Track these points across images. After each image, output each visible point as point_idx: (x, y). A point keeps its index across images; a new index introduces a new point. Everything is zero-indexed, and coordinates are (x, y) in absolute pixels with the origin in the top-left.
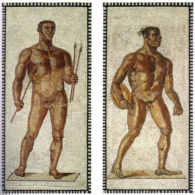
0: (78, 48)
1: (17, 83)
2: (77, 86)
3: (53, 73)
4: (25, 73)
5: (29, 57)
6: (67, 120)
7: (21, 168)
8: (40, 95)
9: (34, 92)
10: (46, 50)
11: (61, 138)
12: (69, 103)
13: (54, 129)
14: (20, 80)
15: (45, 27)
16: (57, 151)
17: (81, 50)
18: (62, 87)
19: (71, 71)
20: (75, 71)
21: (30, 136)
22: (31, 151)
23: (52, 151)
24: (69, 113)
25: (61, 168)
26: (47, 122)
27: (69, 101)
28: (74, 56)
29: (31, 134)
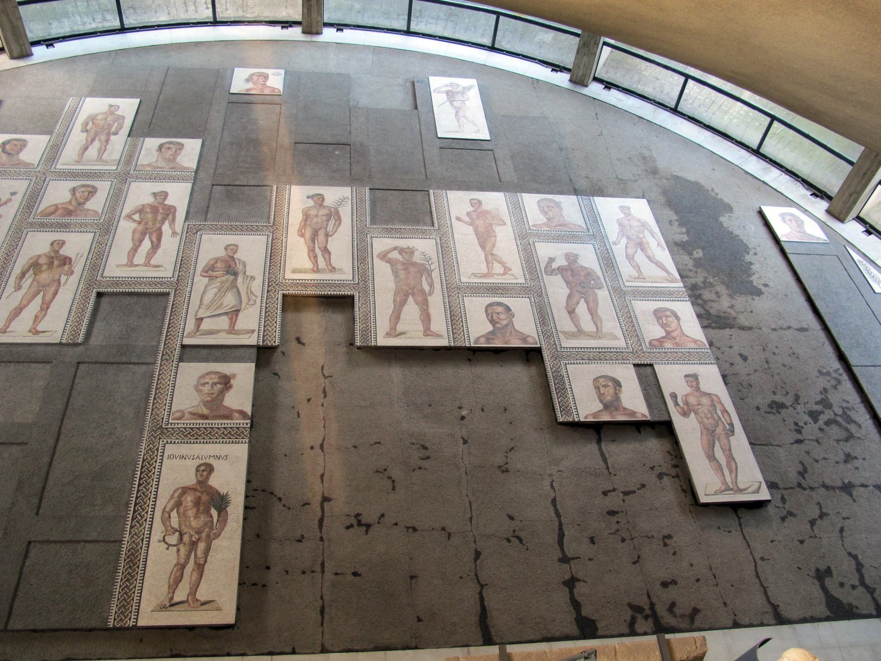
1: (21, 275)
2: (71, 278)
3: (54, 269)
5: (38, 260)
6: (57, 297)
9: (34, 280)
11: (48, 308)
12: (61, 287)
13: (43, 303)
14: (23, 274)
17: (82, 256)
23: (36, 317)
24: (59, 292)
25: (39, 328)
26: (39, 299)
27: (62, 285)
29: (22, 306)
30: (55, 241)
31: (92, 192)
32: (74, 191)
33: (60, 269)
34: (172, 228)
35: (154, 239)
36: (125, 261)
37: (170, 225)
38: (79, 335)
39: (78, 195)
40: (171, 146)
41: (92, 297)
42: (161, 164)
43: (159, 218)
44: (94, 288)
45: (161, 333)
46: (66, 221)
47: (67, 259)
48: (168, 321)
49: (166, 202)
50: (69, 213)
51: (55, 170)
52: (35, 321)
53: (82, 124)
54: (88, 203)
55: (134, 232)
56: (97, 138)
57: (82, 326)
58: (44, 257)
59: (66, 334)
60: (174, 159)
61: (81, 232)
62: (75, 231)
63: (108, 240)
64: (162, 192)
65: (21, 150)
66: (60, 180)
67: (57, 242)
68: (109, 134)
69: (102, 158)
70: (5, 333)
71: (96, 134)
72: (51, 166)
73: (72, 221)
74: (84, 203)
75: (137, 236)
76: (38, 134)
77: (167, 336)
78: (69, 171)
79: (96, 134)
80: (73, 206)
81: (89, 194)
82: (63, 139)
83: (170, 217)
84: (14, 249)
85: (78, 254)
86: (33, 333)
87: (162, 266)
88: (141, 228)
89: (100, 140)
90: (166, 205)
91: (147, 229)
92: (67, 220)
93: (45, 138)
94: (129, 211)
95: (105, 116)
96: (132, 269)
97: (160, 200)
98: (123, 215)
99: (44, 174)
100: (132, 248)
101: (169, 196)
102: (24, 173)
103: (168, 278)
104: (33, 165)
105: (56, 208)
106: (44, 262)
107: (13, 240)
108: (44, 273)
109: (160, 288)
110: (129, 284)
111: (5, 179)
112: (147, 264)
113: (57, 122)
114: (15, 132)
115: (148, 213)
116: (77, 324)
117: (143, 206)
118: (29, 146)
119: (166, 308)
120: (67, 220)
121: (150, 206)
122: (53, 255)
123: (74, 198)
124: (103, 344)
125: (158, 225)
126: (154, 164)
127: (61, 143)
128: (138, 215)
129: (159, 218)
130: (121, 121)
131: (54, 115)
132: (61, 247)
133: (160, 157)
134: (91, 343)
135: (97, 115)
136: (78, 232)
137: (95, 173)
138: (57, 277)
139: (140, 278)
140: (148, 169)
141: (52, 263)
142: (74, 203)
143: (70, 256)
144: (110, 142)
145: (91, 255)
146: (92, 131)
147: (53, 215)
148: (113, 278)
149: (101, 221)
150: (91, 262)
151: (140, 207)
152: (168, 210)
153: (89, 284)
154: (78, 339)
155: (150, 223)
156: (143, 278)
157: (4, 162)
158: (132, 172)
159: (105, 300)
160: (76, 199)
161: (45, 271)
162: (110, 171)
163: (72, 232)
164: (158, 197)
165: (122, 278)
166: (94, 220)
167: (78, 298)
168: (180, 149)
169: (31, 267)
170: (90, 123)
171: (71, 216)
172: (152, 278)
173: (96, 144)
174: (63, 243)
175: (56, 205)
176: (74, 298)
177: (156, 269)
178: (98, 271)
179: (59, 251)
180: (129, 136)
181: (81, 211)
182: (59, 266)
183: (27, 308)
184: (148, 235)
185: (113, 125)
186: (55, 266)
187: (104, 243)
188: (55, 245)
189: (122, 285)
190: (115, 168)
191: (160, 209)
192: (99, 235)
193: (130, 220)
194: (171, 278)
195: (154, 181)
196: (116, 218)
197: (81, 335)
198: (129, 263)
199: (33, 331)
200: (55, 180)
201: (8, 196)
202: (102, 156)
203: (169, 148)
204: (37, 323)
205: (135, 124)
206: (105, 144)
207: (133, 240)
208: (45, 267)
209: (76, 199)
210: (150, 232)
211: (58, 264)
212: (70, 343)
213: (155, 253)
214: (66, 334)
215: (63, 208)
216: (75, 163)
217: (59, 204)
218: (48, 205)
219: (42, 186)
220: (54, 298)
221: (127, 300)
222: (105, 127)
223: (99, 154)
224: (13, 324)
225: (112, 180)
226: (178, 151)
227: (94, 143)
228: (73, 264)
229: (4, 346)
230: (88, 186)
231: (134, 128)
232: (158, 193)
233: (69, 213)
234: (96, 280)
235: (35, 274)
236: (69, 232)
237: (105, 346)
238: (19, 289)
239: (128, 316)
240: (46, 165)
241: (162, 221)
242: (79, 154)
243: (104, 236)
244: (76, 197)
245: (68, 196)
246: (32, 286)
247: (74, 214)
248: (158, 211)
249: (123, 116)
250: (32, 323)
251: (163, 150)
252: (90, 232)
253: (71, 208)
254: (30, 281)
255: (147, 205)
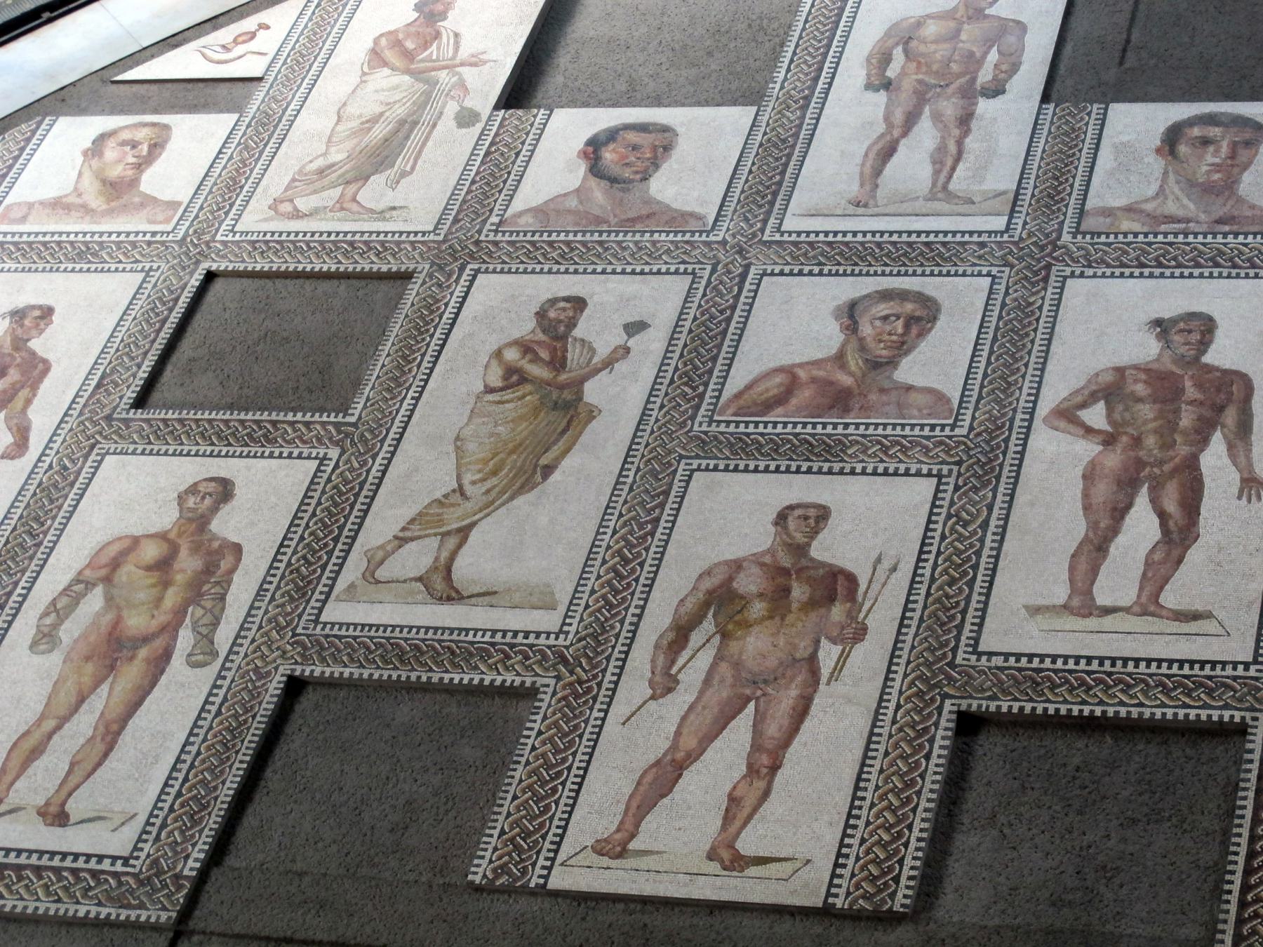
0: (886, 564)
1: (671, 636)
2: (859, 651)
3: (790, 618)
4: (705, 616)
6: (807, 725)
7: (618, 836)
8: (737, 665)
9: (719, 658)
10: (788, 565)
11: (775, 768)
12: (822, 687)
13: (756, 747)
14: (680, 635)
15: (799, 517)
16: (748, 803)
17: (894, 569)
18: (810, 650)
19: (851, 615)
20: (862, 615)
21: (673, 760)
22: (663, 796)
23: (733, 800)
24: (814, 709)
25: (748, 844)
26: (740, 732)
27: (824, 679)
28: (870, 582)
29: (680, 755)
30: (791, 508)
31: (919, 319)
32: (851, 313)
33: (813, 616)
34: (1242, 459)
35: (1171, 506)
36: (1061, 594)
37: (1231, 447)
38: (897, 879)
39: (866, 330)
40: (1215, 132)
41: (940, 733)
42: (1180, 204)
43: (1187, 419)
44: (945, 696)
45: (1218, 892)
46: (829, 429)
47: (841, 580)
48: (1244, 841)
49: (1208, 358)
50: (840, 400)
51: (777, 237)
52: (728, 818)
53: (868, 60)
54: (905, 363)
55: (1089, 476)
56: (927, 109)
57: (906, 845)
58: (755, 570)
59: (846, 872)
60: (1229, 187)
61: (886, 473)
62: (864, 473)
63: (990, 508)
64: (1192, 316)
65: (655, 164)
66: (800, 273)
67: (798, 512)
68: (970, 94)
69: (951, 187)
70: (620, 856)
71: (922, 97)
72: (765, 222)
73: (851, 430)
74: (892, 363)
75: (1103, 491)
76: (707, 103)
77: (1243, 904)
78: (830, 238)
79: (922, 97)
80: (851, 374)
81: (907, 326)
82: (803, 117)
83: (1230, 416)
84: (644, 537)
85: (879, 560)
86: (722, 862)
87: (1208, 615)
88: (1114, 460)
89: (937, 117)
90: (1209, 369)
91: (1140, 464)
92: (830, 426)
93: (741, 116)
94: (1064, 394)
95: (952, 24)
96: (1092, 623)
97: (1183, 350)
98: (1044, 409)
99: (740, 252)
100: (1086, 539)
101: (1220, 334)
102: (668, 252)
103: (1235, 665)
104: (699, 218)
105: (791, 379)
106: (753, 589)
107: (642, 504)
108: (756, 629)
109: (1205, 706)
110: (1083, 683)
111: (604, 272)
112: (1149, 605)
113: (775, 56)
114: (629, 99)
115: (1140, 400)
116: (886, 837)
117: (1120, 371)
118: (683, 147)
119: (1232, 789)
120: (830, 426)
121: (1147, 371)
122: (786, 561)
123: (853, 344)
124: (991, 924)
125: (1183, 450)
126: (1149, 207)
127: (796, 135)
128: (1100, 407)
129: (1187, 419)
130: (1011, 39)
131: (761, 28)
132: (815, 532)
133: (1172, 178)
134: (940, 914)
135: (919, 24)
136: (875, 473)
137: (927, 244)
138: (803, 651)
139: (1125, 660)
140: (1126, 225)
141: (787, 591)
142: (854, 362)
143: (849, 566)
144: (974, 124)
145: (929, 565)
146: (908, 85)
147: (780, 410)
148: (1018, 656)
149: (957, 431)
150: (928, 594)
151: (1108, 378)
152: (1219, 390)
153: (926, 681)
154: (893, 896)
155: (1150, 441)
156: (1137, 661)
157: (597, 212)
158: (1066, 238)
159: (990, 746)
160: (863, 348)
161: (759, 621)
162: (984, 238)
163: (853, 472)
164: (1177, 338)
165: (1054, 658)
166: (933, 427)
167: (885, 731)
168: (1248, 144)
169: (706, 605)
170: (898, 53)
171: (846, 410)
172: (1171, 662)
173: (925, 135)
174: (822, 514)
175: (789, 371)
176: (872, 734)
177: (1193, 627)
178: (960, 628)
179: (809, 545)
180: (1046, 98)
181: (882, 391)
182: (811, 604)
183: (697, 765)
184: (1144, 490)
185: (980, 62)
186: (795, 606)
187: (974, 518)
188: (792, 524)
189: (1053, 687)
190: (999, 223)
191: (1188, 384)
192: (957, 488)
193: (1071, 428)
194: (1247, 666)
195: (1157, 271)
196: (1017, 423)
197: (903, 881)
198: (1076, 602)
199: (726, 855)
200: (782, 273)
201: (619, 338)
202: (950, 177)
203: (1205, 142)
204: (738, 823)
205: (1068, 49)
206: (956, 132)
207: (1087, 508)
208: (758, 609)
209: (863, 348)
210: (1151, 477)
211: (805, 598)
212: (863, 909)
213: (1180, 561)
214: (846, 872)
215: (814, 380)
216: (851, 209)
217: (801, 365)
218: (758, 369)
219: (737, 297)
220: (794, 729)
221: (1078, 750)
222: (955, 67)
223: (937, 173)
224: (649, 823)
225: (994, 271)
226: (1243, 155)
227: (916, 129)
228: (860, 599)
229: (621, 906)
230: (903, 295)
231: (1062, 69)
232: (1174, 321)
233: (840, 400)
234: (952, 665)
235: (725, 635)
236: (841, 473)
237: (997, 931)
238: (670, 690)
239: (1080, 813)
240: (746, 220)
241: (1197, 431)
242: (862, 174)
243: (976, 490)
244: (861, 340)
245: (830, 337)
246: (717, 678)
247: (856, 403)
248: (1177, 393)
249: (1018, 22)
250: (719, 823)
251: (1183, 149)
252: (919, 474)
253: (846, 380)
254: (704, 660)
255: (1136, 367)
